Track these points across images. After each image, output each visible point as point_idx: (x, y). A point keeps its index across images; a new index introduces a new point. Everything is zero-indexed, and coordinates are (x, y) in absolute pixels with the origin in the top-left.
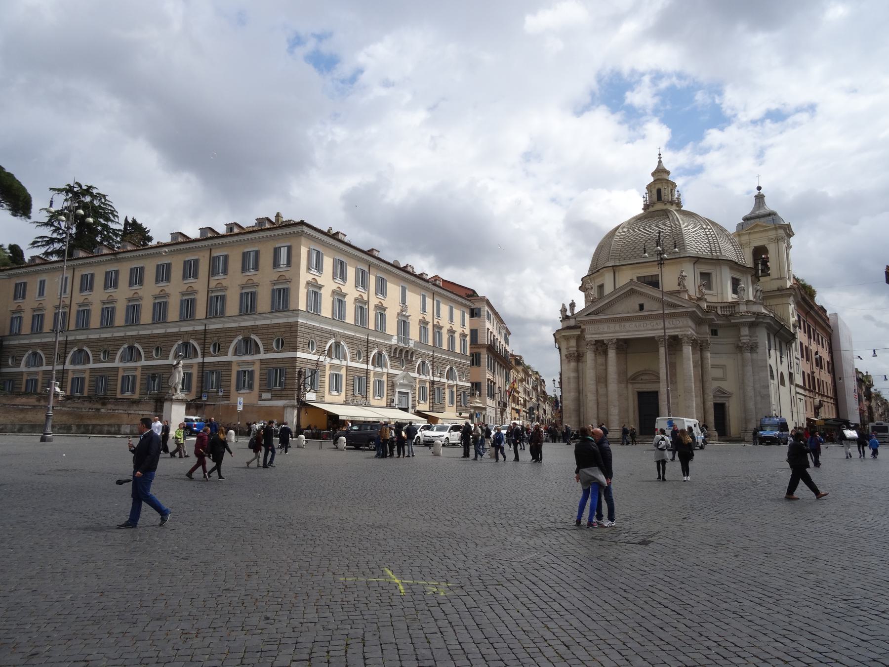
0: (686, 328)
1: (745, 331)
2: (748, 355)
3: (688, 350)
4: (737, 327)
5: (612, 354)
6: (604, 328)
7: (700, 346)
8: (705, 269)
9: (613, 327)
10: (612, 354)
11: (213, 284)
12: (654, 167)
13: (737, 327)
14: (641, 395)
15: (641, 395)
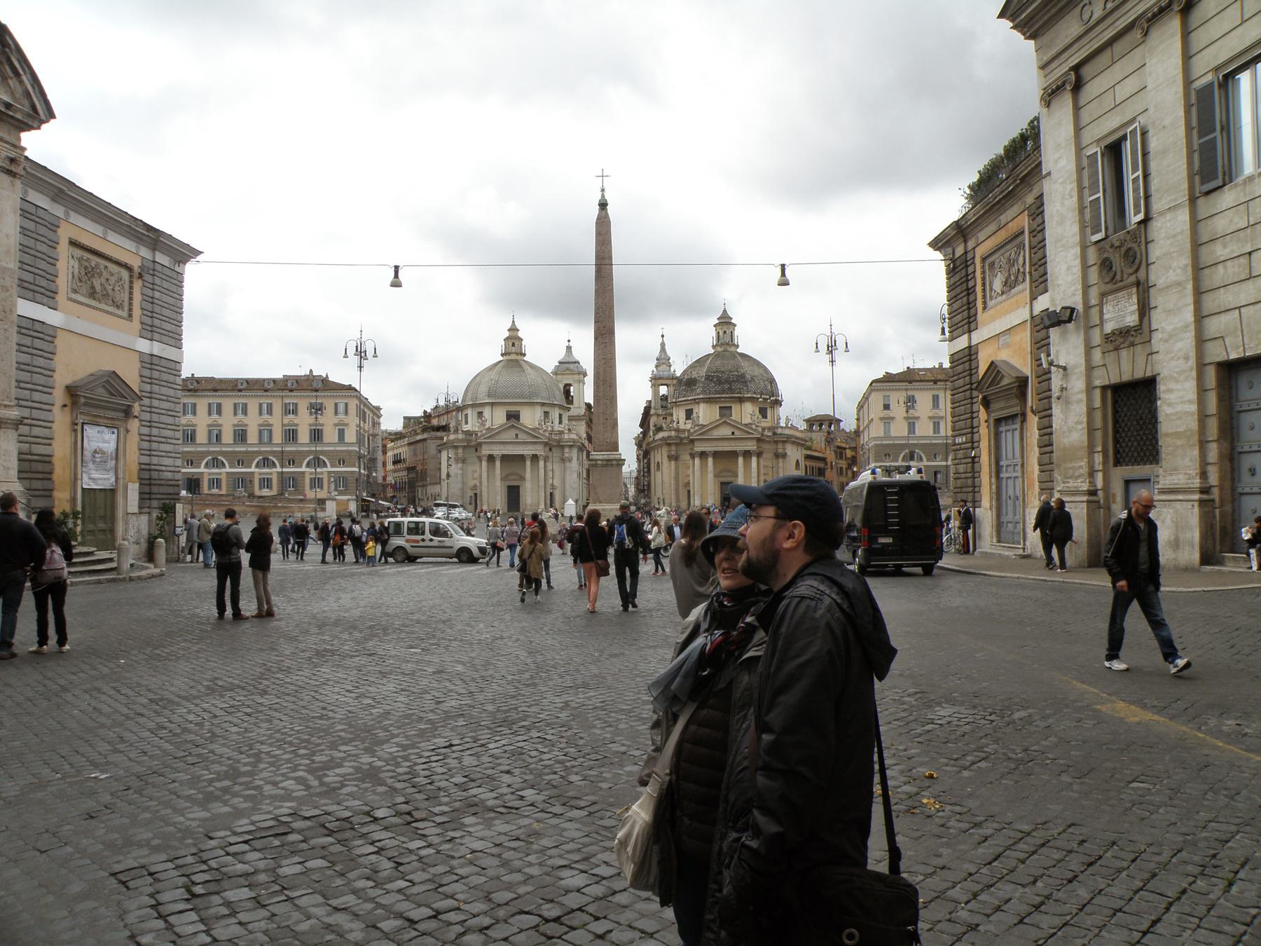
0: (540, 451)
1: (567, 450)
2: (568, 464)
3: (541, 463)
4: (563, 447)
5: (498, 463)
6: (494, 447)
7: (546, 459)
8: (547, 409)
9: (499, 447)
10: (498, 463)
11: (286, 422)
12: (509, 326)
13: (563, 447)
14: (510, 488)
15: (510, 488)
